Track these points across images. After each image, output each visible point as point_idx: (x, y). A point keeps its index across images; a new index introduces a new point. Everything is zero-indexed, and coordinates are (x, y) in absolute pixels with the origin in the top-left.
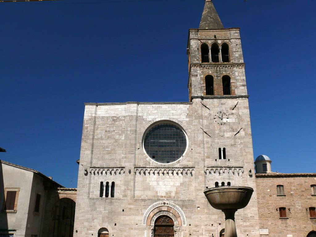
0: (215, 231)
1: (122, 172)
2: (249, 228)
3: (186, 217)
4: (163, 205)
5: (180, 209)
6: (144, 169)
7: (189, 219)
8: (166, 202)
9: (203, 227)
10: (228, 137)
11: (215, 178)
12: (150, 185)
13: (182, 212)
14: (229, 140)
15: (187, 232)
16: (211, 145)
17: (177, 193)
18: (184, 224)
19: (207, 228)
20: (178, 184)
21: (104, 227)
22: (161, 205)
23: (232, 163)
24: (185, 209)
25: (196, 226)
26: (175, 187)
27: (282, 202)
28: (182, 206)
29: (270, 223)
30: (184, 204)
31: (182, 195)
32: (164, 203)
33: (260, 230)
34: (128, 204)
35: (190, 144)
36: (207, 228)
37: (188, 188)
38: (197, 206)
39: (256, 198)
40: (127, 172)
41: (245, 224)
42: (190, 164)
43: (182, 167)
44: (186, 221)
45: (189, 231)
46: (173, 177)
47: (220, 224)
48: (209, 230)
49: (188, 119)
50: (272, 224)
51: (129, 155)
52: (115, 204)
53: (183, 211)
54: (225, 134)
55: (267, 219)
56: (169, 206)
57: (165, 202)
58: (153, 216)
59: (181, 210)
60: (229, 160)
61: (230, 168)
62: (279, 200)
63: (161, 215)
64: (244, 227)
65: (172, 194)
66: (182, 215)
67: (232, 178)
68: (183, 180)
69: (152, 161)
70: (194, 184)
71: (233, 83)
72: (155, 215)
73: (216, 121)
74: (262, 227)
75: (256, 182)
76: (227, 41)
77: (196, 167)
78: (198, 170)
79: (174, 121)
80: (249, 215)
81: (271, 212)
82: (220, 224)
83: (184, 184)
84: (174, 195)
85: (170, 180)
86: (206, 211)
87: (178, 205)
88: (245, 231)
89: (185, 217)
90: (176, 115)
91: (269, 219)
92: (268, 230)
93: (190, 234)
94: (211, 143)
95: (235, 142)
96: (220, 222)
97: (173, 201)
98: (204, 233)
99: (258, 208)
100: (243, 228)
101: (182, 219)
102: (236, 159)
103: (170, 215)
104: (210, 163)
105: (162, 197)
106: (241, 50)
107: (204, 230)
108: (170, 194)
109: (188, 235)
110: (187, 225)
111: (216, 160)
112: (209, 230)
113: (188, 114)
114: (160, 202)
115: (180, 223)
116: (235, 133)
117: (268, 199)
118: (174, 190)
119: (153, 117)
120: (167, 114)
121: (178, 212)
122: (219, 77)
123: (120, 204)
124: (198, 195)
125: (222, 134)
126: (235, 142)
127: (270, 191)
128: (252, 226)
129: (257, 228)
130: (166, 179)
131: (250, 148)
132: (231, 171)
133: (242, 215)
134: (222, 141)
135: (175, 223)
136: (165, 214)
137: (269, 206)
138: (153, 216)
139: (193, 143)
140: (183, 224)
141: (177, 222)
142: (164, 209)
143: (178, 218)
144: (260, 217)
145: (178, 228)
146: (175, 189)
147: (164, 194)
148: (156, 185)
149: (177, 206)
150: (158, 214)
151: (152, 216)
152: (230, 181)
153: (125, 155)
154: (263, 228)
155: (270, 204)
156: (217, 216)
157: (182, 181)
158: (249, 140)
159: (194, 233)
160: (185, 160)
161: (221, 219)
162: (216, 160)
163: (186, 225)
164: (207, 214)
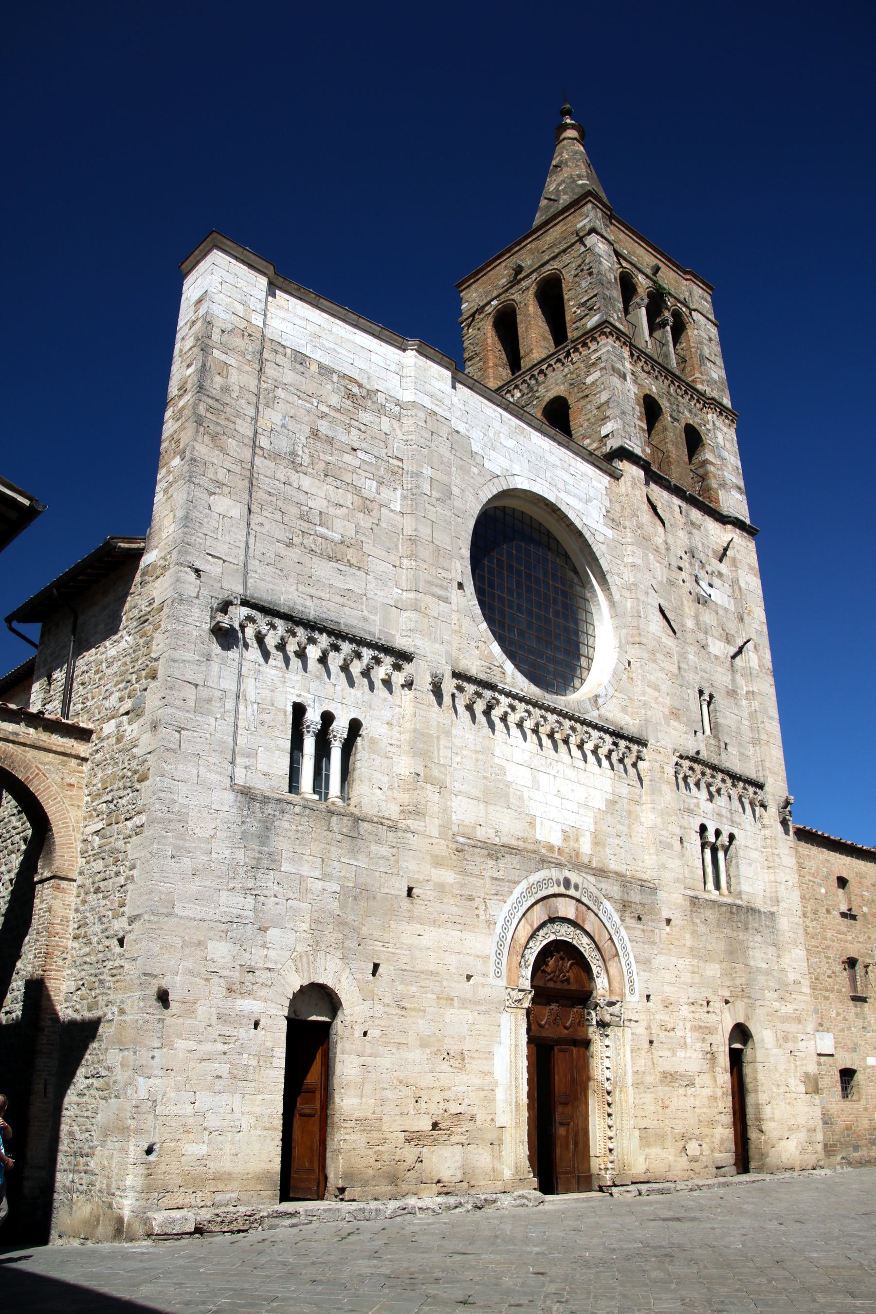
0: (716, 1029)
1: (398, 679)
2: (792, 1027)
4: (562, 890)
5: (616, 917)
6: (488, 694)
7: (644, 971)
8: (574, 878)
9: (685, 1011)
10: (716, 657)
11: (697, 805)
12: (509, 778)
13: (623, 932)
14: (719, 669)
15: (640, 1029)
16: (679, 668)
17: (598, 842)
18: (632, 990)
19: (697, 1016)
20: (600, 803)
21: (321, 981)
23: (732, 761)
25: (667, 1005)
26: (591, 814)
27: (850, 938)
28: (624, 906)
29: (834, 1014)
30: (626, 897)
31: (612, 857)
32: (567, 883)
33: (817, 1033)
34: (428, 857)
35: (623, 641)
36: (697, 1016)
37: (629, 827)
38: (665, 914)
39: (800, 913)
40: (424, 683)
41: (784, 1010)
42: (629, 723)
43: (612, 728)
44: (635, 977)
45: (648, 1028)
46: (581, 764)
47: (727, 1002)
48: (702, 1024)
49: (609, 533)
50: (838, 1014)
51: (429, 599)
52: (374, 848)
53: (626, 928)
54: (710, 639)
55: (827, 994)
56: (584, 900)
58: (528, 942)
59: (619, 922)
60: (726, 744)
61: (735, 778)
62: (846, 929)
63: (553, 937)
64: (785, 1019)
65: (582, 840)
67: (737, 819)
68: (613, 787)
69: (509, 666)
70: (648, 817)
71: (712, 464)
72: (532, 936)
73: (684, 581)
74: (821, 1026)
75: (797, 852)
76: (684, 309)
77: (651, 741)
78: (659, 758)
79: (572, 516)
80: (792, 976)
81: (833, 972)
82: (727, 1002)
83: (617, 807)
84: (589, 852)
85: (571, 774)
86: (689, 941)
87: (609, 899)
88: (786, 1039)
89: (632, 959)
90: (575, 496)
91: (831, 996)
92: (831, 1035)
93: (651, 1042)
94: (679, 662)
95: (733, 680)
96: (726, 994)
97: (592, 879)
98: (689, 1040)
99: (807, 950)
100: (780, 1026)
101: (625, 969)
102: (742, 750)
103: (583, 943)
104: (682, 741)
105: (551, 848)
106: (719, 361)
107: (688, 1025)
108: (577, 840)
109: (646, 1045)
110: (640, 996)
111: (695, 732)
112: (700, 1027)
113: (608, 512)
114: (555, 874)
115: (616, 985)
116: (733, 650)
117: (825, 921)
118: (587, 823)
119: (505, 463)
120: (549, 480)
121: (612, 932)
122: (678, 421)
123: (394, 851)
124: (663, 867)
125: (701, 636)
126: (733, 680)
127: (827, 893)
128: (799, 1020)
129: (810, 1027)
130: (560, 766)
131: (771, 718)
132: (734, 793)
133: (775, 973)
134: (703, 666)
135: (601, 984)
136: (564, 933)
137: (828, 947)
138: (528, 942)
139: (631, 640)
140: (627, 991)
141: (606, 981)
142: (567, 909)
143: (610, 960)
144: (814, 988)
145: (615, 1009)
146: (592, 821)
147: (556, 840)
148: (530, 784)
149: (607, 904)
150: (541, 933)
151: (523, 941)
152: (735, 832)
153: (412, 595)
154: (820, 1028)
155: (828, 942)
156: (718, 967)
157: (610, 790)
158: (766, 687)
159: (663, 1034)
160: (614, 700)
161: (728, 983)
162: (695, 732)
163: (636, 998)
164: (694, 957)
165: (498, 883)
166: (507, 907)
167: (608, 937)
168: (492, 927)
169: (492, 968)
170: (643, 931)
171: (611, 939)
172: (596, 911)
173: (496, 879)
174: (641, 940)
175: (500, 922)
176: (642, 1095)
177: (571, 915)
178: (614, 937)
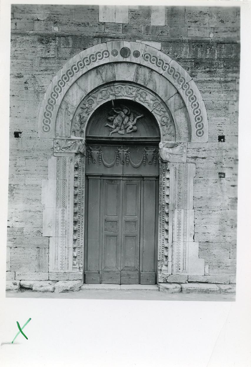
3: (208, 108)
4: (120, 58)
5: (186, 74)
13: (193, 85)
18: (200, 133)
22: (112, 59)
24: (206, 77)
32: (125, 52)
44: (205, 122)
53: (196, 82)
56: (145, 63)
57: (126, 44)
66: (194, 98)
110: (210, 137)
114: (109, 46)
121: (179, 87)
165: (47, 61)
166: (56, 78)
167: (175, 92)
168: (41, 95)
169: (39, 123)
170: (220, 82)
171: (178, 93)
172: (161, 72)
173: (46, 58)
174: (216, 90)
175: (49, 89)
176: (204, 216)
177: (130, 78)
178: (181, 91)
